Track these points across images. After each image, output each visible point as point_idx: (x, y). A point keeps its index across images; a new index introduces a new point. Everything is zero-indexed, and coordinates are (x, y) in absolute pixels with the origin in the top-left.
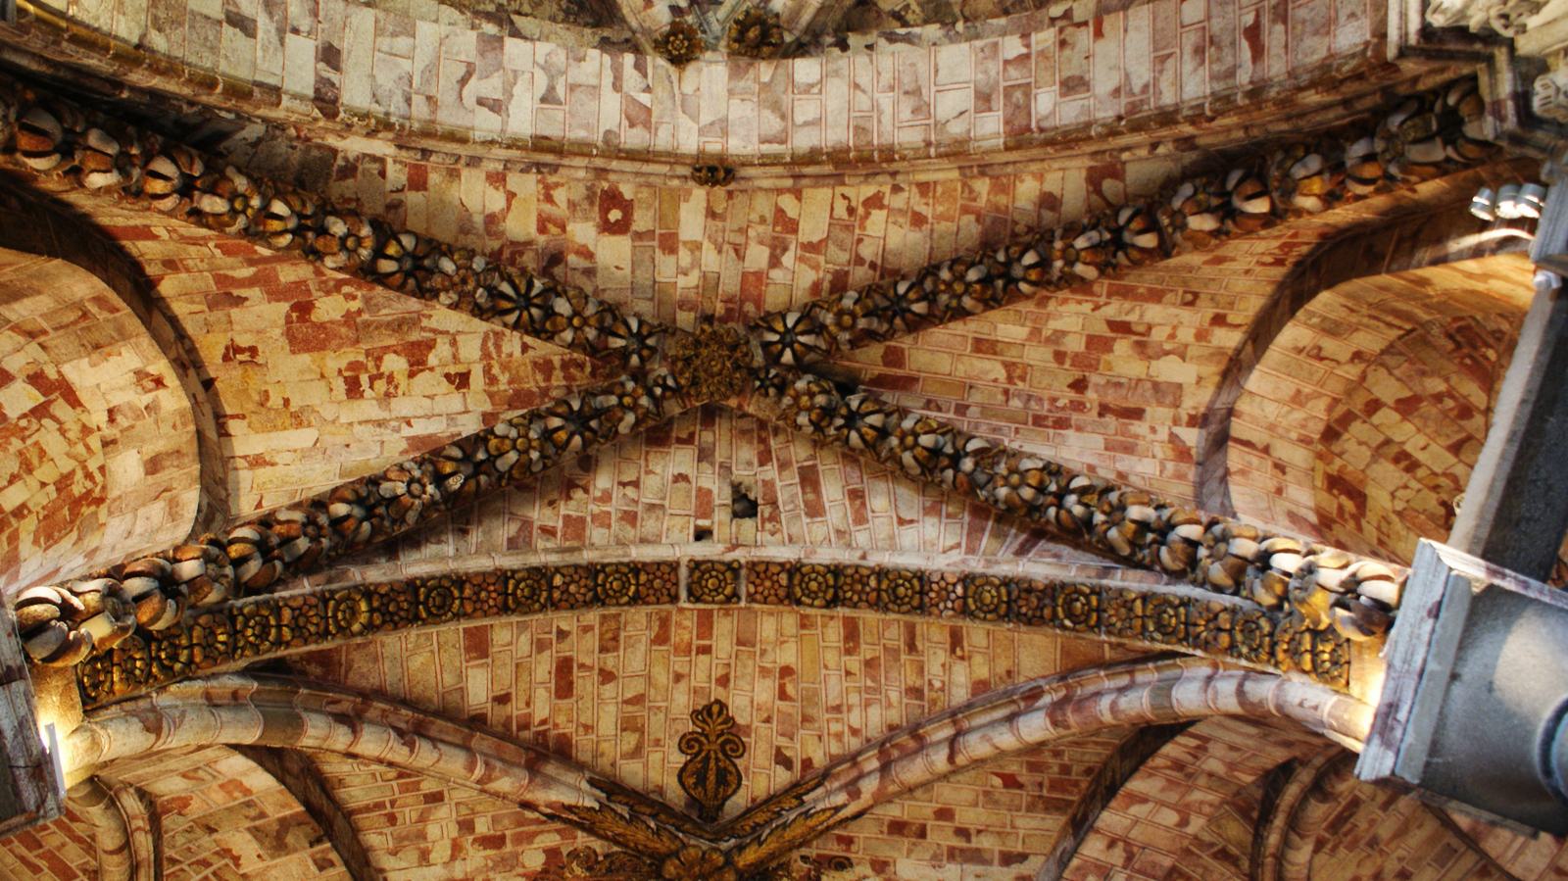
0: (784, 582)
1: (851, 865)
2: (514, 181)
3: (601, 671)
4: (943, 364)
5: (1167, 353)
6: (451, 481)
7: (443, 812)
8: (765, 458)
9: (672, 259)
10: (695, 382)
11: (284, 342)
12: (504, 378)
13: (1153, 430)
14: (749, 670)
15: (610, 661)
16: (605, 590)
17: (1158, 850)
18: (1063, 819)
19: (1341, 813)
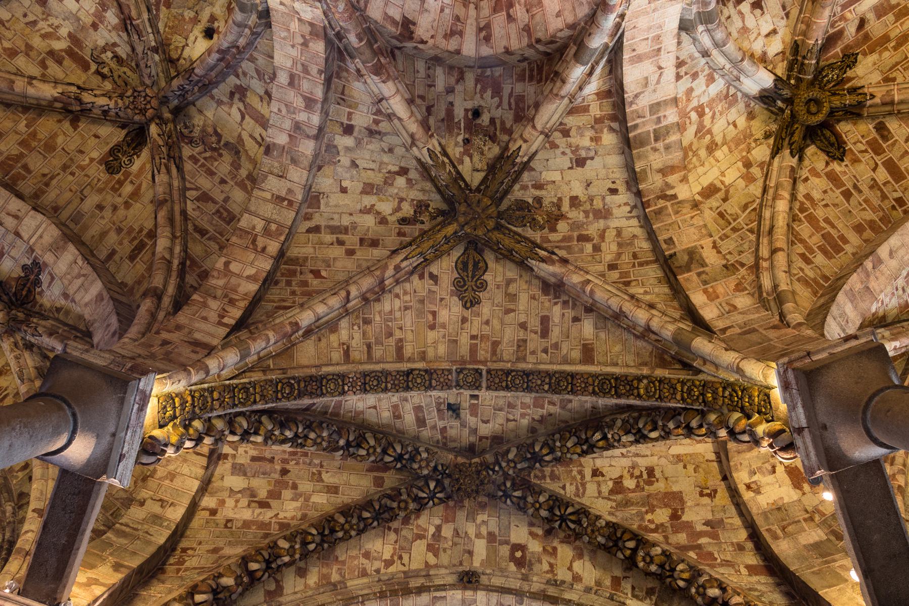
0: (434, 382)
1: (398, 221)
2: (568, 577)
3: (526, 330)
4: (354, 479)
5: (239, 492)
6: (599, 437)
7: (608, 258)
8: (444, 430)
9: (491, 529)
10: (478, 473)
11: (686, 498)
12: (575, 473)
13: (246, 452)
14: (451, 327)
15: (522, 334)
16: (523, 379)
17: (240, 246)
18: (288, 254)
19: (139, 253)
